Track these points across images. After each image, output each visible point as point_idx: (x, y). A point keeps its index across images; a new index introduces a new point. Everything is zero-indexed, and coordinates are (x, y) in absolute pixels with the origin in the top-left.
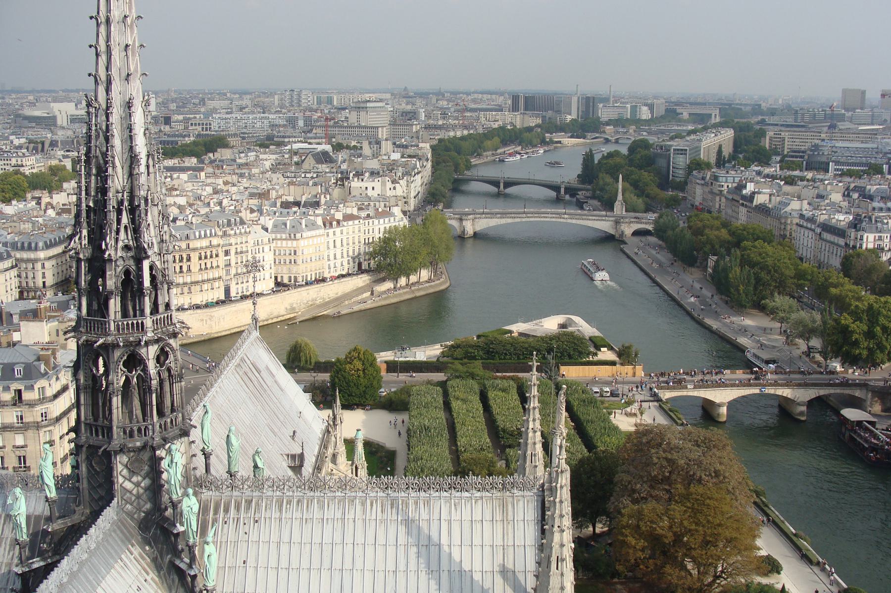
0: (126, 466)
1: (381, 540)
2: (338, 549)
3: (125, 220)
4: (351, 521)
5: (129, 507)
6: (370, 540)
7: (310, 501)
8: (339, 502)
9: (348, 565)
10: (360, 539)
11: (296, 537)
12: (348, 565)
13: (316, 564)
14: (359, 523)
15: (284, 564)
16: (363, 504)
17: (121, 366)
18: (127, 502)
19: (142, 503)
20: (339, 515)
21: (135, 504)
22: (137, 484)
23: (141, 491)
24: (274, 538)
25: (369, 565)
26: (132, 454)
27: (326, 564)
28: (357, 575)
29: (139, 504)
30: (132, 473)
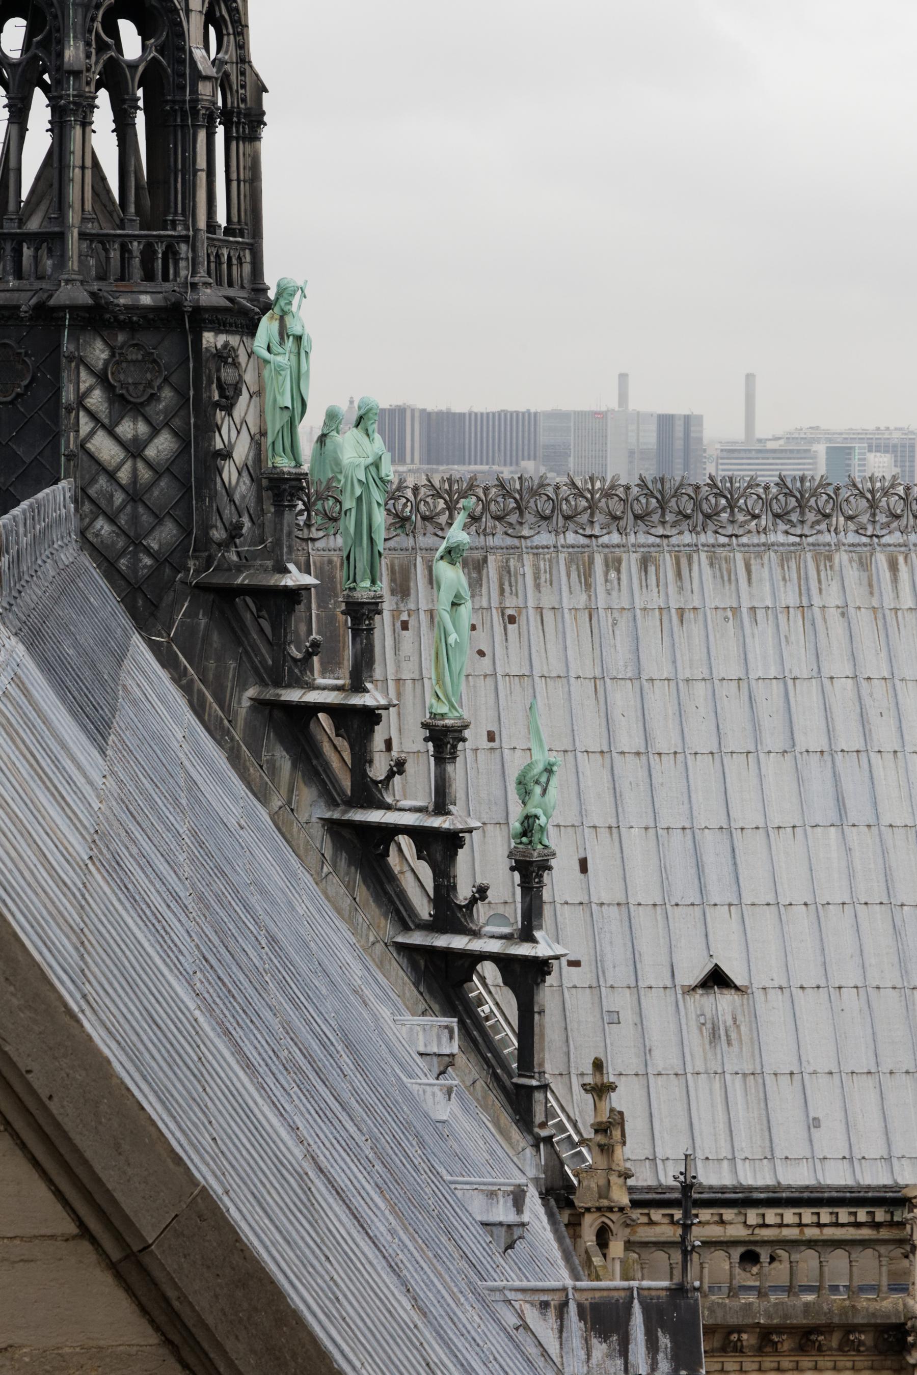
0: (102, 378)
4: (833, 614)
5: (102, 526)
7: (683, 559)
8: (783, 561)
11: (656, 663)
13: (736, 740)
14: (863, 621)
15: (628, 738)
16: (864, 565)
17: (98, 25)
18: (99, 510)
19: (146, 518)
20: (790, 597)
21: (123, 520)
22: (134, 450)
23: (145, 474)
24: (582, 664)
26: (121, 338)
29: (134, 519)
30: (124, 403)
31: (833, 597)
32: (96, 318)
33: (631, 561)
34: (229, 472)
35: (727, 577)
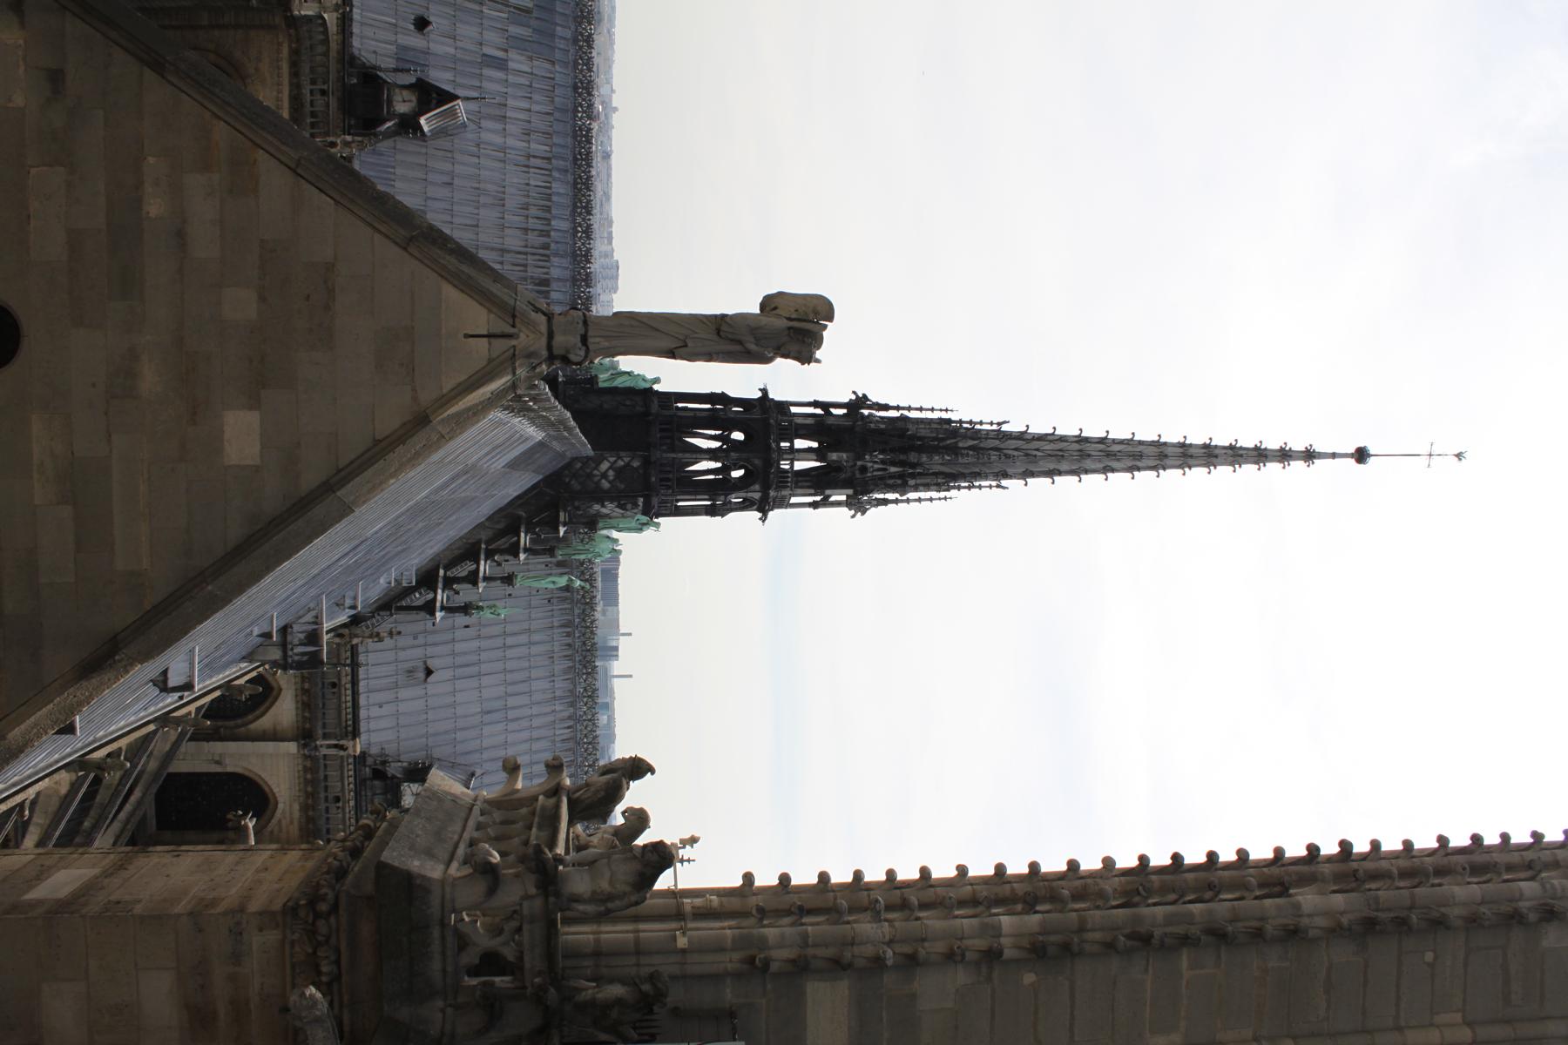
0: (628, 465)
1: (536, 746)
2: (524, 700)
3: (893, 469)
5: (579, 465)
6: (535, 734)
9: (511, 714)
10: (536, 722)
11: (534, 650)
12: (511, 714)
13: (510, 677)
14: (551, 718)
16: (570, 718)
22: (604, 476)
24: (534, 625)
25: (510, 738)
27: (510, 689)
28: (500, 727)
30: (620, 472)
31: (558, 708)
32: (647, 462)
33: (569, 640)
34: (597, 507)
35: (565, 672)
